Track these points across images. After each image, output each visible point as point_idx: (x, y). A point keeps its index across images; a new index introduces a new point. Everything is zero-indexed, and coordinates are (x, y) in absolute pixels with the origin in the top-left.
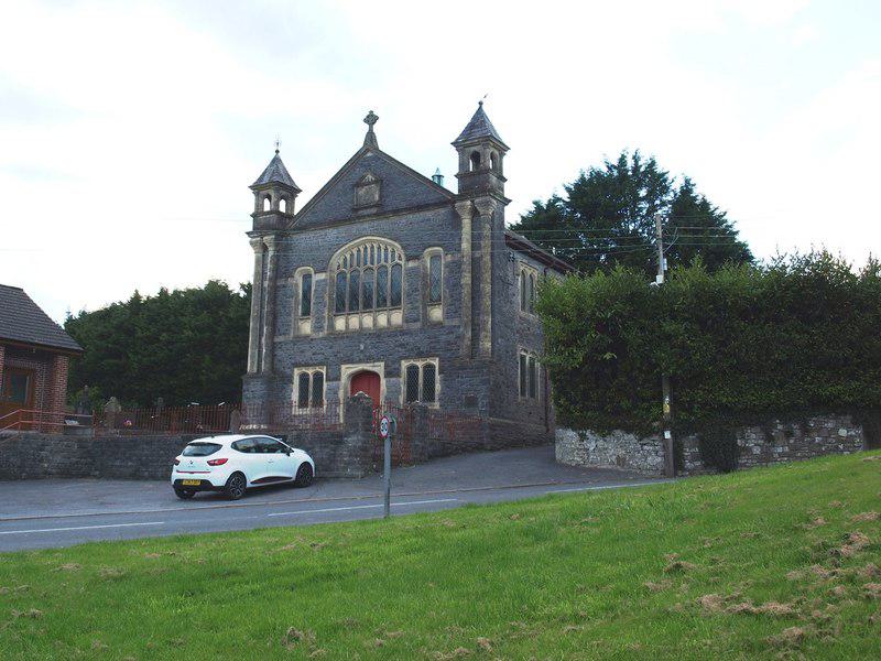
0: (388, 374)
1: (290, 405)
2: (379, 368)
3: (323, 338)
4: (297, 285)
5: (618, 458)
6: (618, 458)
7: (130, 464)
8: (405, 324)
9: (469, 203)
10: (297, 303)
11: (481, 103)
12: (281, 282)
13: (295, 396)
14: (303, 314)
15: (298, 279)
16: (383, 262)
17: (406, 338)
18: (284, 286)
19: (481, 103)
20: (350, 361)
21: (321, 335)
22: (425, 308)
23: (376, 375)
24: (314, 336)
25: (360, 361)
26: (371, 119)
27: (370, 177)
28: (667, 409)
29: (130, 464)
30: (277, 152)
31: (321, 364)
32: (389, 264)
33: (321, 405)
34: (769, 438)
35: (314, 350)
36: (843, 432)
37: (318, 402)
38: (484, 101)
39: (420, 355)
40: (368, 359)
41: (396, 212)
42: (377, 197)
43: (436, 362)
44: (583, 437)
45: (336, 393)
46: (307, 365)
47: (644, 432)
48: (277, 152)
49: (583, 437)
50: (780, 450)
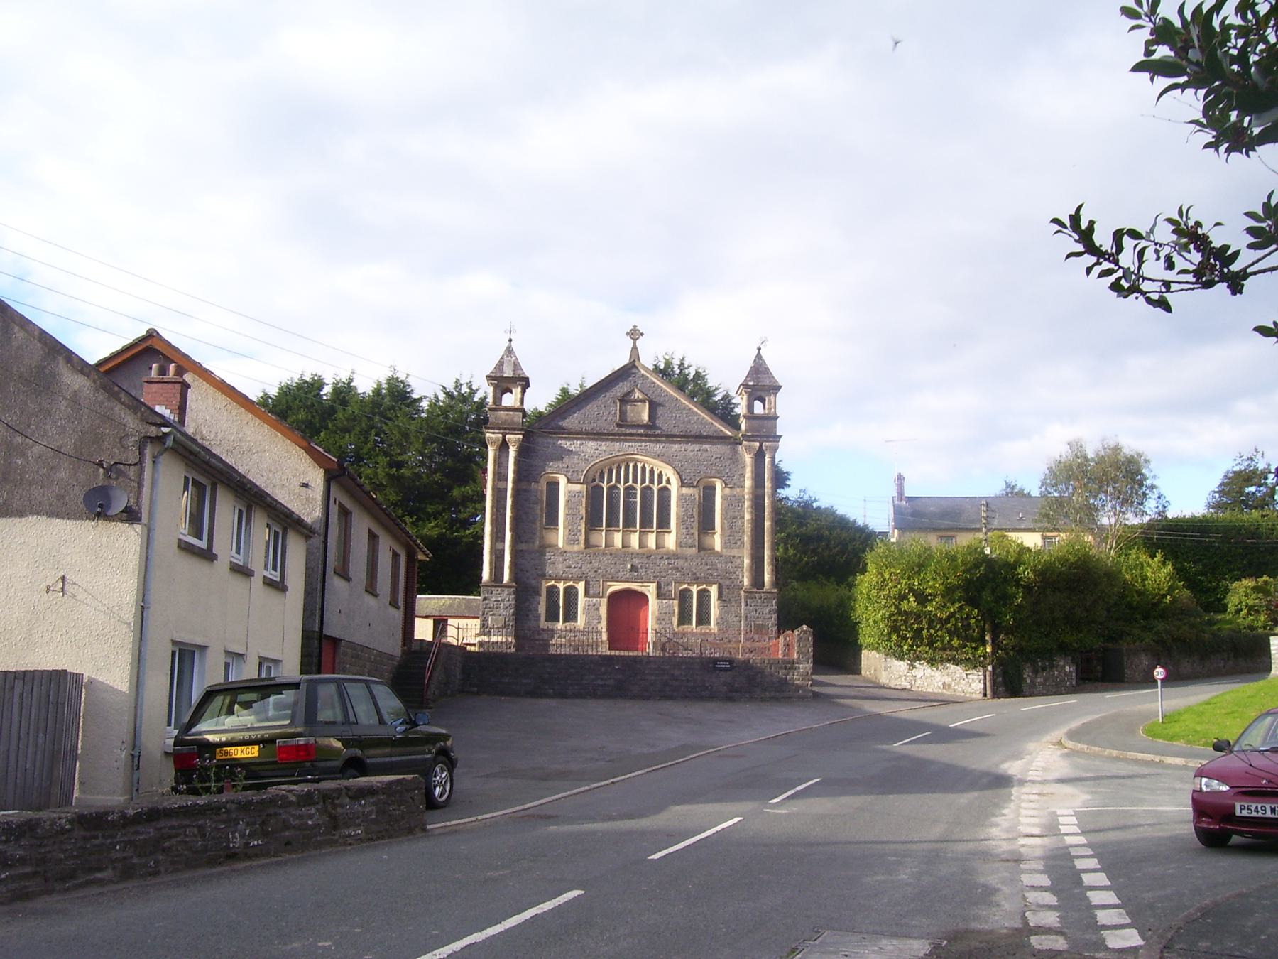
0: (660, 595)
1: (538, 617)
2: (650, 590)
3: (578, 552)
4: (542, 491)
5: (944, 684)
6: (944, 684)
7: (525, 681)
8: (679, 549)
9: (757, 444)
10: (542, 509)
11: (759, 349)
12: (524, 485)
13: (542, 609)
14: (547, 523)
15: (543, 486)
16: (631, 482)
17: (680, 563)
18: (525, 491)
19: (759, 349)
20: (613, 579)
21: (576, 548)
22: (699, 535)
23: (643, 598)
24: (568, 548)
25: (627, 581)
26: (635, 334)
27: (638, 395)
28: (989, 650)
29: (525, 681)
30: (510, 340)
31: (577, 580)
32: (655, 488)
33: (575, 619)
34: (1036, 672)
35: (567, 563)
36: (1067, 669)
37: (570, 616)
38: (762, 347)
39: (696, 580)
40: (638, 579)
41: (671, 438)
42: (645, 417)
43: (714, 590)
44: (912, 666)
45: (598, 609)
46: (558, 579)
47: (971, 663)
48: (510, 340)
49: (912, 666)
50: (1039, 680)
